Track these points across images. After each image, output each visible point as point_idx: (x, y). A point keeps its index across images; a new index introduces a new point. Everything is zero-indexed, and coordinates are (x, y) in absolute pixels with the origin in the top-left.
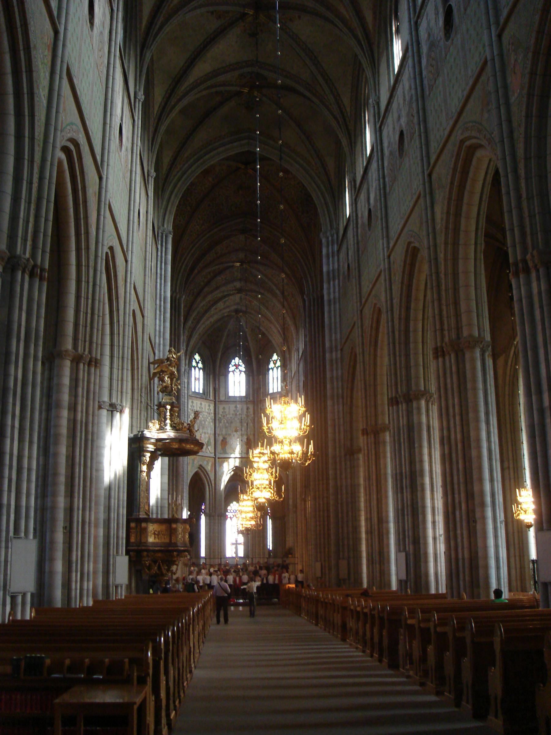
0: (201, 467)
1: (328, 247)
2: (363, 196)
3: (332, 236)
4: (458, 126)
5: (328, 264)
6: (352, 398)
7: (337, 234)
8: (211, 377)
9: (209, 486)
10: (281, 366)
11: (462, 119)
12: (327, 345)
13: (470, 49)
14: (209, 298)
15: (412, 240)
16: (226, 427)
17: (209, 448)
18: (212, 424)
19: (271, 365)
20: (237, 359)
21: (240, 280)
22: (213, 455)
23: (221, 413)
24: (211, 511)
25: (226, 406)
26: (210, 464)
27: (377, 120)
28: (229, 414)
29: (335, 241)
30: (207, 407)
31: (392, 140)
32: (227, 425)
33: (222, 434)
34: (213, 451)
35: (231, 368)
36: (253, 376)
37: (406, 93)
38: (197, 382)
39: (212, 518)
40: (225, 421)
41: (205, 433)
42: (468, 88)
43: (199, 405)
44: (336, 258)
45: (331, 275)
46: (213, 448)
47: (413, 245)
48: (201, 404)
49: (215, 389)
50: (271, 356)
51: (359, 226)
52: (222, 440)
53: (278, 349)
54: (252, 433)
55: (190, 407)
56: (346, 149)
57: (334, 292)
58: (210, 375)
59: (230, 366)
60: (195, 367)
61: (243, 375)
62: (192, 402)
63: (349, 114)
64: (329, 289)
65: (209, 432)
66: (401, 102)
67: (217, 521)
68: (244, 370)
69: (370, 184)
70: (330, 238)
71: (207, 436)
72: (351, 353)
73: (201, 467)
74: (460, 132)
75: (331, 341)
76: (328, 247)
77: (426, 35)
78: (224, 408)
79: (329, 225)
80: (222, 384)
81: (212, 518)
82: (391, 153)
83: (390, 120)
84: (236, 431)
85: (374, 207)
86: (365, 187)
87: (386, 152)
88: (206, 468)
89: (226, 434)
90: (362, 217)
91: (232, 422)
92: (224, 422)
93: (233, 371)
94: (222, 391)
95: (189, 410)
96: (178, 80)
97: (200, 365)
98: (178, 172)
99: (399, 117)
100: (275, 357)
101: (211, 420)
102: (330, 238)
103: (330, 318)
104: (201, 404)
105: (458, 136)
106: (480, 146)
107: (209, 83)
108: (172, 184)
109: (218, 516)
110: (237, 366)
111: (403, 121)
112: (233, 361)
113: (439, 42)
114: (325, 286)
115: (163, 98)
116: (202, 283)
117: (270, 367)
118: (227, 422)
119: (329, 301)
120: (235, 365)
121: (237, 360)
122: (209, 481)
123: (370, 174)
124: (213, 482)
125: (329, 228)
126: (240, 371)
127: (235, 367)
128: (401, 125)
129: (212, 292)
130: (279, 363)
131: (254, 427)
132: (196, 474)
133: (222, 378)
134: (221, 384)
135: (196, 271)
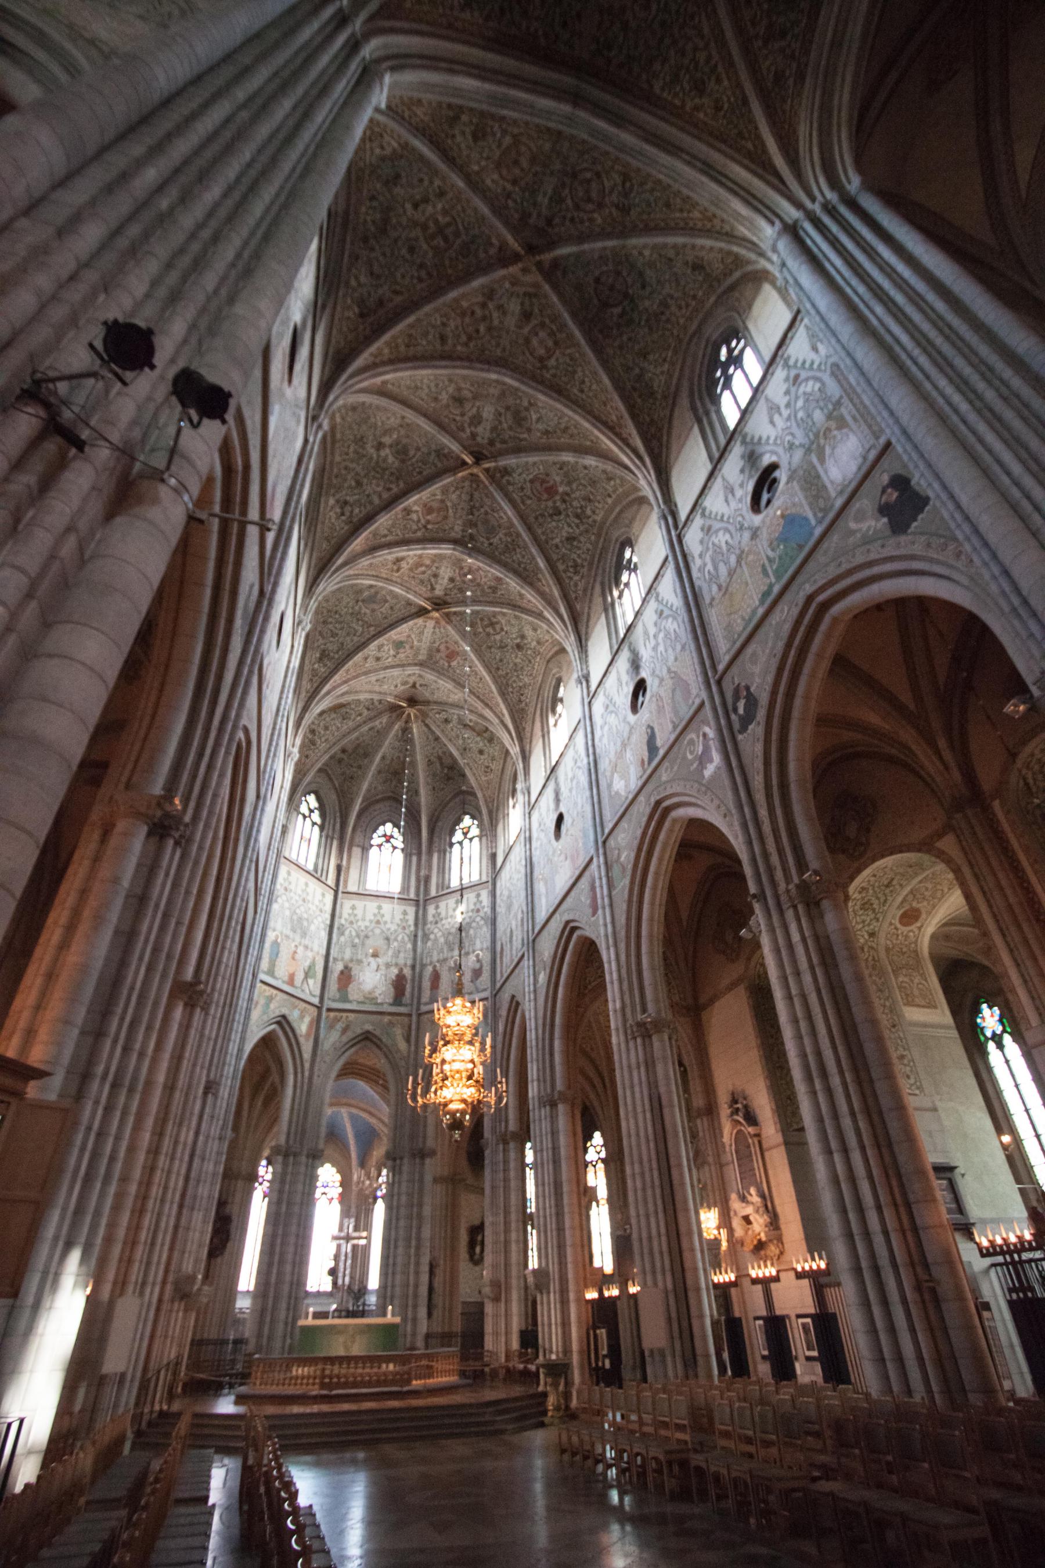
0: (283, 1021)
8: (335, 843)
16: (354, 946)
17: (311, 981)
18: (324, 935)
19: (458, 836)
22: (316, 1001)
23: (345, 915)
24: (291, 1142)
25: (360, 903)
26: (307, 1020)
28: (364, 920)
30: (319, 897)
32: (357, 941)
34: (318, 992)
35: (376, 840)
36: (419, 854)
38: (304, 845)
41: (306, 947)
43: (302, 885)
46: (319, 985)
48: (307, 884)
49: (339, 868)
50: (459, 820)
52: (342, 972)
54: (409, 962)
55: (280, 879)
58: (332, 839)
59: (375, 835)
60: (305, 817)
61: (399, 857)
62: (289, 873)
65: (316, 948)
67: (302, 1169)
68: (402, 846)
71: (310, 954)
73: (283, 1021)
78: (353, 908)
81: (291, 1159)
84: (375, 955)
88: (295, 1025)
89: (352, 960)
91: (367, 937)
92: (351, 936)
93: (380, 846)
94: (354, 874)
95: (278, 886)
97: (316, 817)
100: (467, 821)
101: (322, 926)
104: (307, 884)
109: (308, 1157)
110: (388, 838)
112: (381, 828)
116: (376, 501)
118: (358, 936)
120: (385, 836)
124: (307, 1065)
126: (395, 848)
130: (475, 831)
131: (415, 950)
132: (267, 1042)
133: (357, 851)
134: (353, 860)
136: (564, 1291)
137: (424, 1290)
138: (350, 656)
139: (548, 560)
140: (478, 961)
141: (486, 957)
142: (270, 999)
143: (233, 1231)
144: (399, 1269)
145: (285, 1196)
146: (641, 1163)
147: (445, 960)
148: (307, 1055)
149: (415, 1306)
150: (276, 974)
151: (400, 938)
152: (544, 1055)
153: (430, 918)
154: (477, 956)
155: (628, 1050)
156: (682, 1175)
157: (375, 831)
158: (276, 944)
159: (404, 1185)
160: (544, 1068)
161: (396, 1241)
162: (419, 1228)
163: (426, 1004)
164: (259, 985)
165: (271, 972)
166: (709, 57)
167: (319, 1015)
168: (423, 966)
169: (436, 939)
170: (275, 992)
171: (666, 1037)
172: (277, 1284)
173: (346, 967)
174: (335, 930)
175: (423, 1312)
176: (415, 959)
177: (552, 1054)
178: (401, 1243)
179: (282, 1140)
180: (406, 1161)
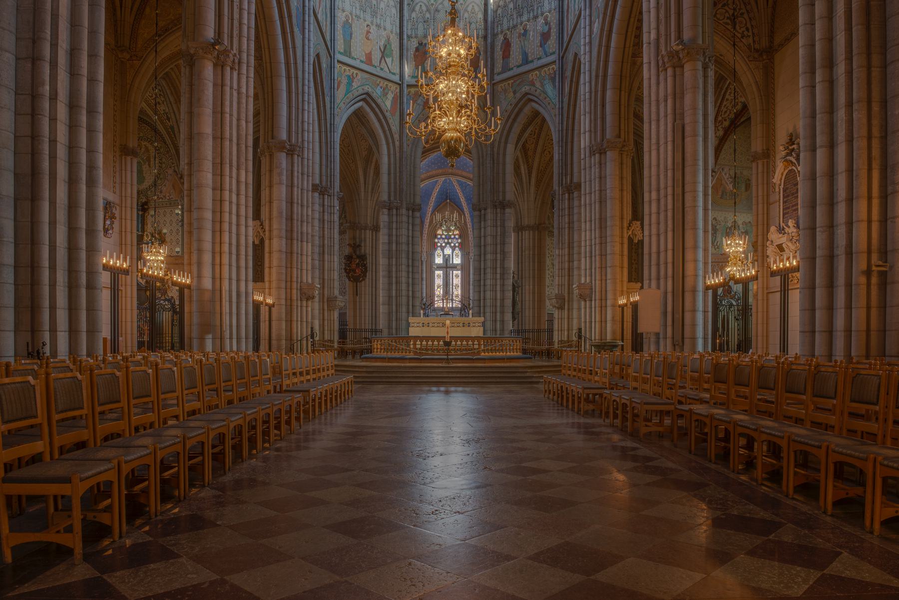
9: (388, 144)
18: (395, 12)
22: (396, 78)
24: (392, 198)
26: (390, 96)
32: (428, 15)
33: (416, 37)
39: (394, 211)
40: (424, 8)
41: (378, 26)
52: (417, 49)
65: (389, 27)
67: (405, 219)
71: (384, 33)
73: (367, 98)
88: (379, 101)
109: (408, 209)
118: (428, 10)
122: (389, 136)
124: (396, 137)
132: (358, 117)
136: (603, 299)
137: (509, 302)
140: (546, 23)
141: (553, 18)
142: (351, 79)
143: (369, 265)
144: (488, 288)
145: (394, 238)
146: (658, 190)
147: (515, 27)
148: (395, 128)
149: (502, 313)
150: (353, 54)
151: (469, 9)
152: (596, 106)
154: (546, 19)
155: (658, 83)
156: (695, 199)
158: (347, 25)
159: (489, 229)
160: (596, 120)
161: (485, 269)
162: (503, 260)
163: (499, 74)
164: (337, 65)
165: (347, 53)
167: (401, 91)
168: (494, 35)
170: (355, 71)
171: (699, 65)
172: (396, 297)
173: (421, 44)
174: (406, 7)
175: (508, 316)
176: (486, 29)
177: (603, 106)
178: (488, 270)
179: (385, 197)
180: (489, 210)
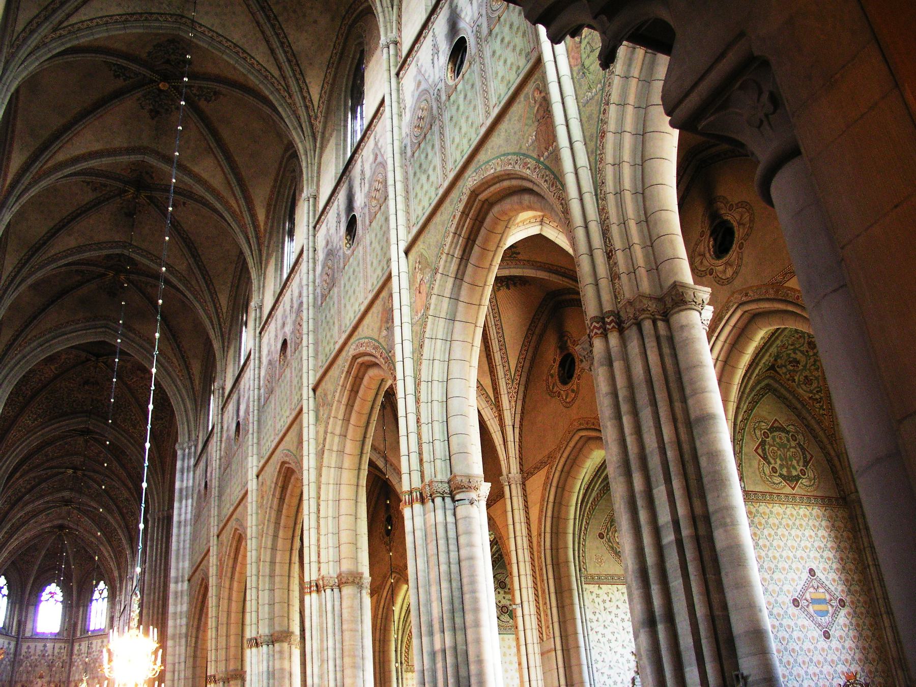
1: (183, 460)
2: (231, 407)
3: (190, 448)
4: (352, 340)
5: (182, 481)
6: (197, 638)
7: (196, 446)
10: (108, 597)
11: (356, 333)
12: (173, 573)
13: (372, 263)
14: (29, 508)
15: (287, 459)
19: (96, 595)
20: (54, 585)
21: (71, 490)
27: (257, 325)
29: (193, 454)
31: (273, 348)
35: (45, 596)
36: (71, 606)
37: (295, 300)
42: (366, 302)
44: (192, 473)
45: (184, 493)
47: (287, 465)
51: (224, 439)
53: (106, 576)
56: (218, 355)
57: (186, 513)
59: (44, 594)
61: (59, 607)
63: (224, 315)
64: (180, 509)
66: (288, 307)
68: (61, 599)
69: (242, 393)
70: (187, 451)
72: (201, 585)
74: (353, 347)
75: (177, 569)
76: (183, 460)
77: (324, 243)
79: (187, 436)
80: (30, 615)
82: (270, 363)
83: (272, 327)
85: (244, 419)
86: (235, 397)
87: (265, 361)
90: (228, 430)
96: (35, 249)
98: (16, 355)
99: (284, 324)
100: (102, 585)
102: (187, 451)
103: (178, 542)
105: (351, 350)
106: (375, 365)
107: (70, 259)
108: (7, 368)
110: (52, 594)
111: (288, 329)
113: (338, 251)
114: (176, 505)
115: (14, 268)
116: (23, 490)
117: (94, 598)
119: (180, 522)
121: (53, 587)
123: (242, 383)
125: (187, 440)
127: (50, 595)
128: (285, 332)
129: (33, 502)
130: (105, 594)
135: (18, 474)
138: (18, 529)
139: (118, 507)
153: (75, 651)
157: (44, 590)
166: (136, 419)
169: (78, 666)
